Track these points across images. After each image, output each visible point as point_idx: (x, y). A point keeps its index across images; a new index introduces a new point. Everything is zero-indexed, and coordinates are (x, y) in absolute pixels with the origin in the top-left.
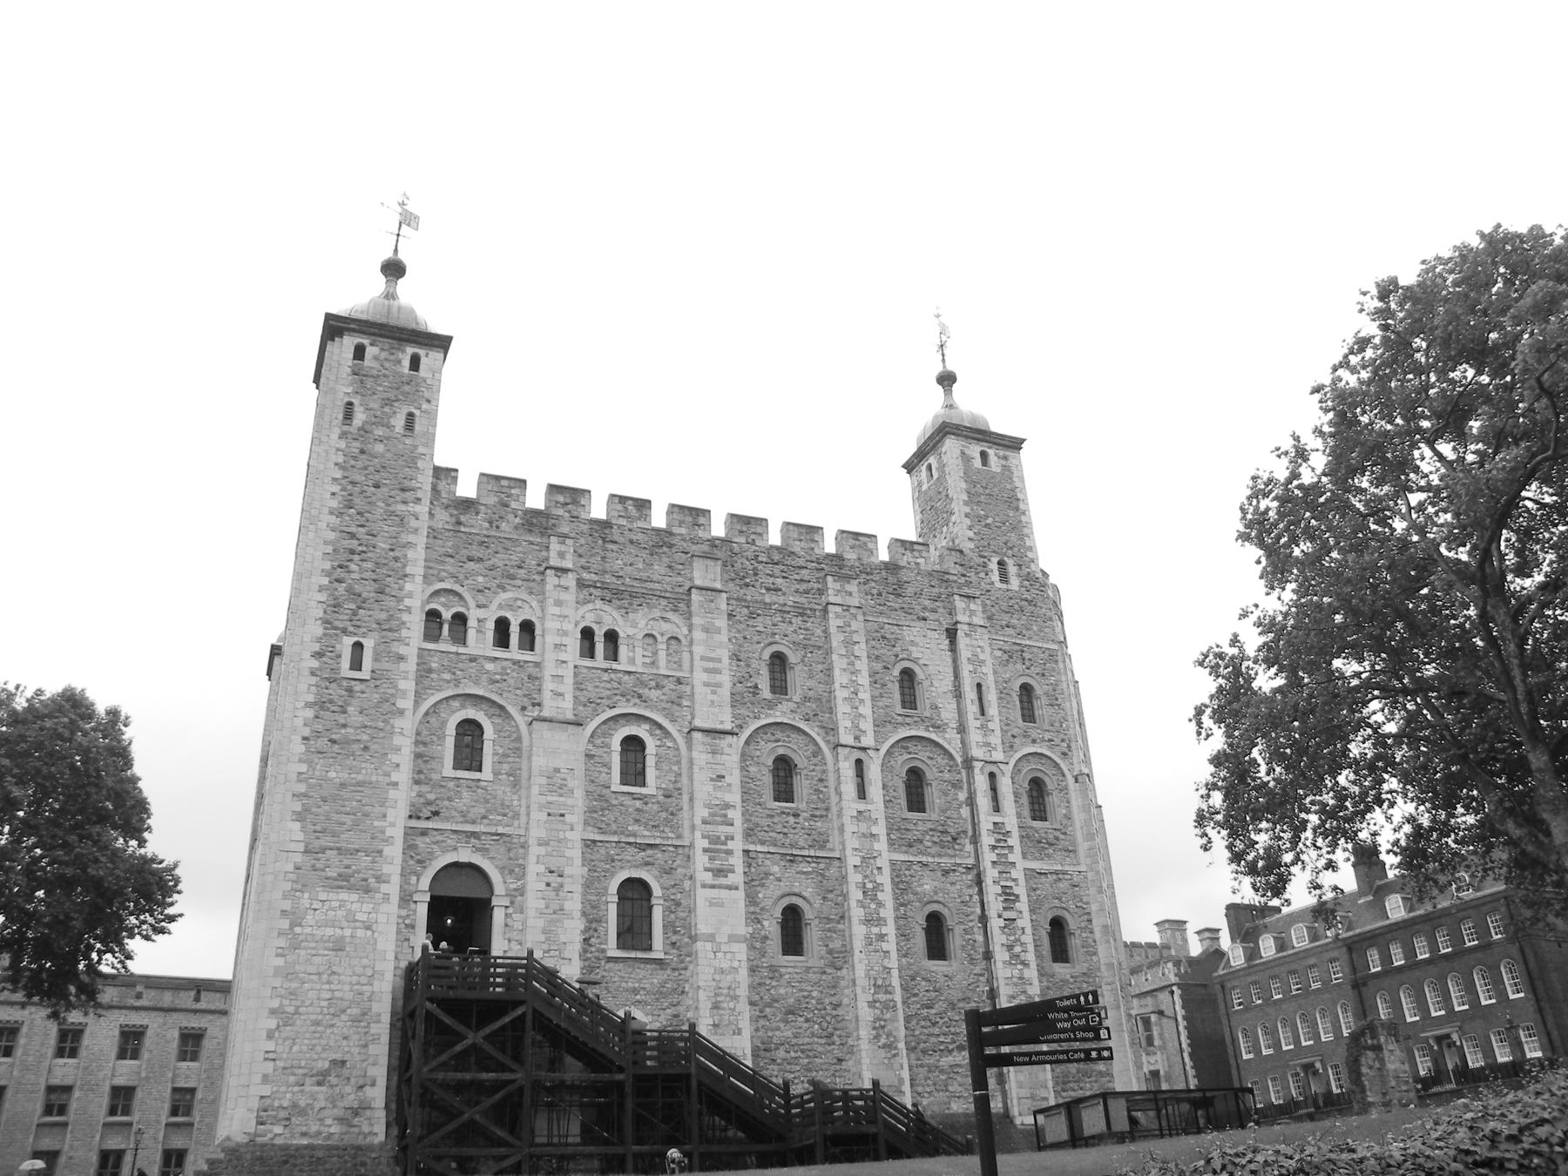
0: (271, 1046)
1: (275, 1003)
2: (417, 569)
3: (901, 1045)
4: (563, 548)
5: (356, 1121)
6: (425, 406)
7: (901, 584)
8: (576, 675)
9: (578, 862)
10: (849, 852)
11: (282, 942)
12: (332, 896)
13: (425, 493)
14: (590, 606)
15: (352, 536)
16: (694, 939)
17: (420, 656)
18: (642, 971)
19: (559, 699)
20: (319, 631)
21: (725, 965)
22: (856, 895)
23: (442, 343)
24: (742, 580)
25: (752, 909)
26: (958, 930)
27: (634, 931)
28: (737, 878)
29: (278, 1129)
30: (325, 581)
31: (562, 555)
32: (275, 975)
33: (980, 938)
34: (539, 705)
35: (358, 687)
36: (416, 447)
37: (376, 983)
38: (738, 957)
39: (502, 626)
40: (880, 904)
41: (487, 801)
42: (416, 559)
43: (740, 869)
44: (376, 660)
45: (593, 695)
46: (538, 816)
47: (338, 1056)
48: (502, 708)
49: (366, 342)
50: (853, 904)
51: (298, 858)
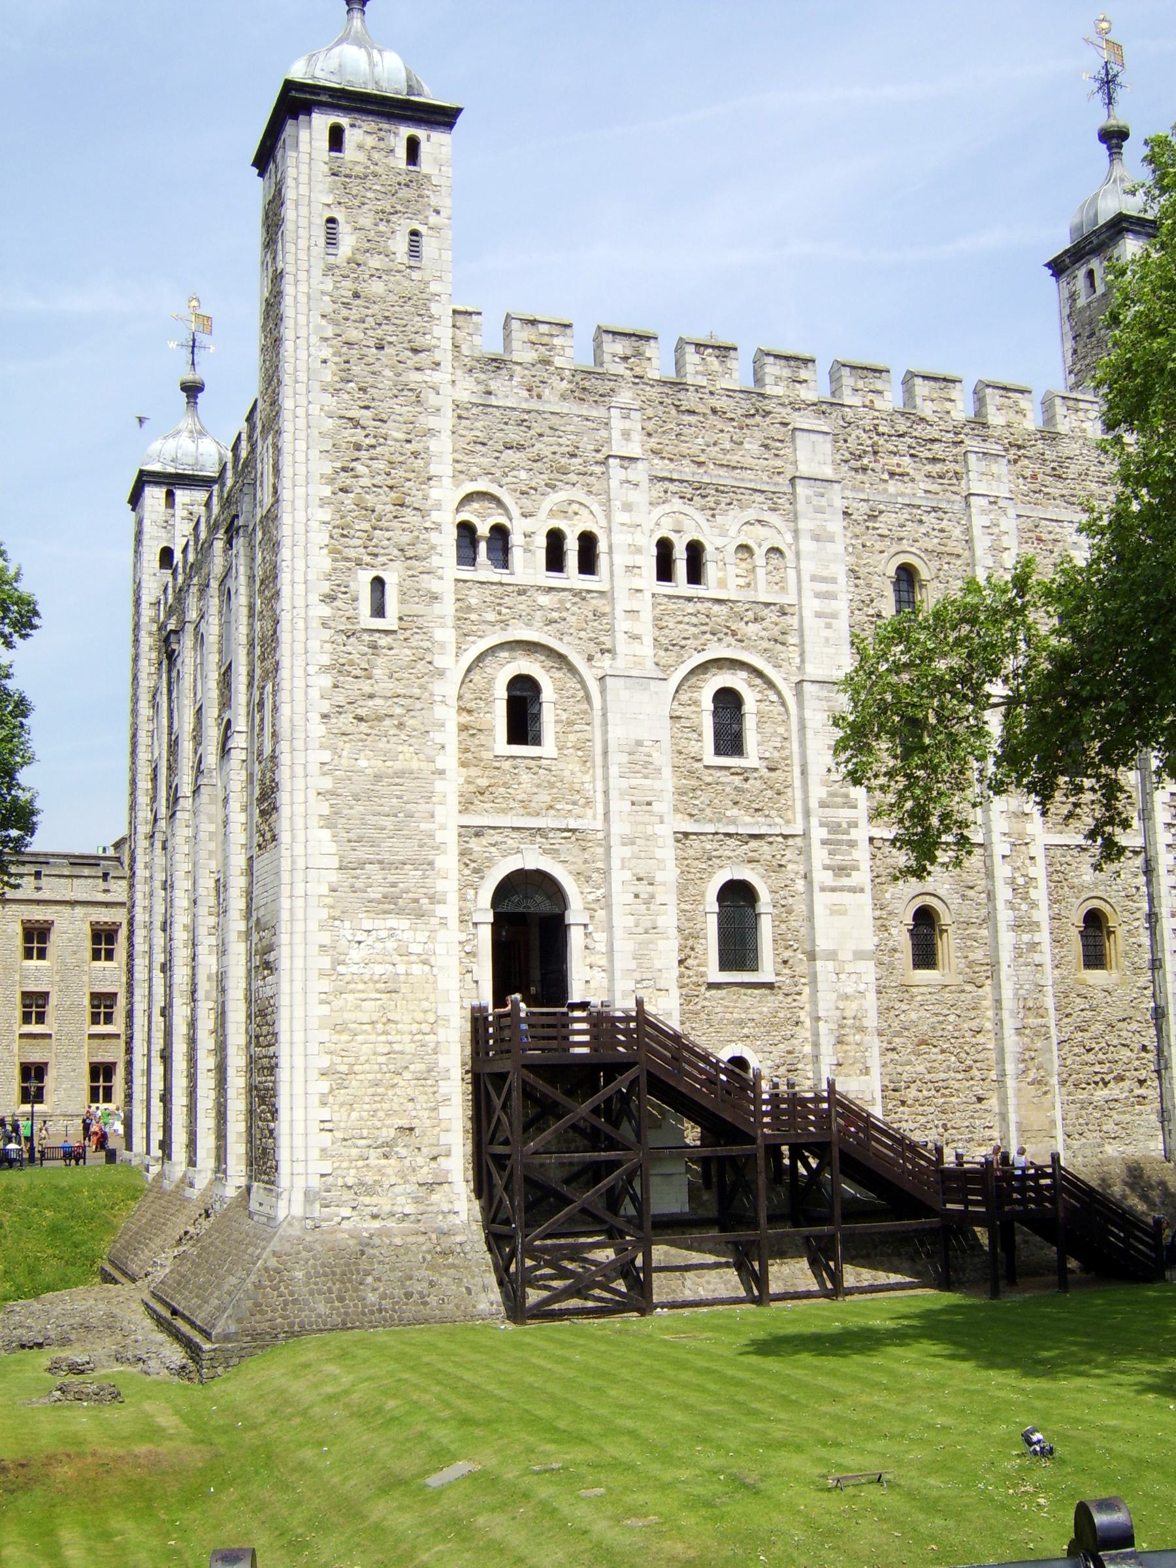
0: (325, 1114)
1: (325, 1062)
2: (442, 467)
3: (1054, 1080)
4: (627, 424)
5: (435, 1197)
6: (433, 219)
7: (1062, 462)
8: (654, 605)
9: (671, 864)
10: (996, 837)
11: (325, 985)
12: (379, 923)
13: (444, 354)
14: (667, 508)
15: (356, 424)
16: (812, 956)
17: (457, 591)
18: (750, 998)
19: (635, 648)
20: (324, 562)
21: (850, 990)
22: (1003, 893)
23: (444, 118)
24: (857, 462)
25: (878, 913)
26: (1120, 931)
27: (738, 948)
28: (862, 877)
29: (346, 1212)
30: (327, 491)
31: (626, 435)
32: (320, 1027)
33: (1146, 941)
34: (609, 651)
35: (384, 641)
36: (427, 283)
37: (441, 1031)
38: (865, 978)
39: (555, 539)
40: (1034, 905)
41: (551, 785)
42: (442, 449)
43: (865, 864)
44: (402, 602)
45: (674, 634)
46: (619, 806)
47: (405, 1123)
48: (562, 658)
49: (344, 121)
50: (1000, 905)
51: (334, 877)
